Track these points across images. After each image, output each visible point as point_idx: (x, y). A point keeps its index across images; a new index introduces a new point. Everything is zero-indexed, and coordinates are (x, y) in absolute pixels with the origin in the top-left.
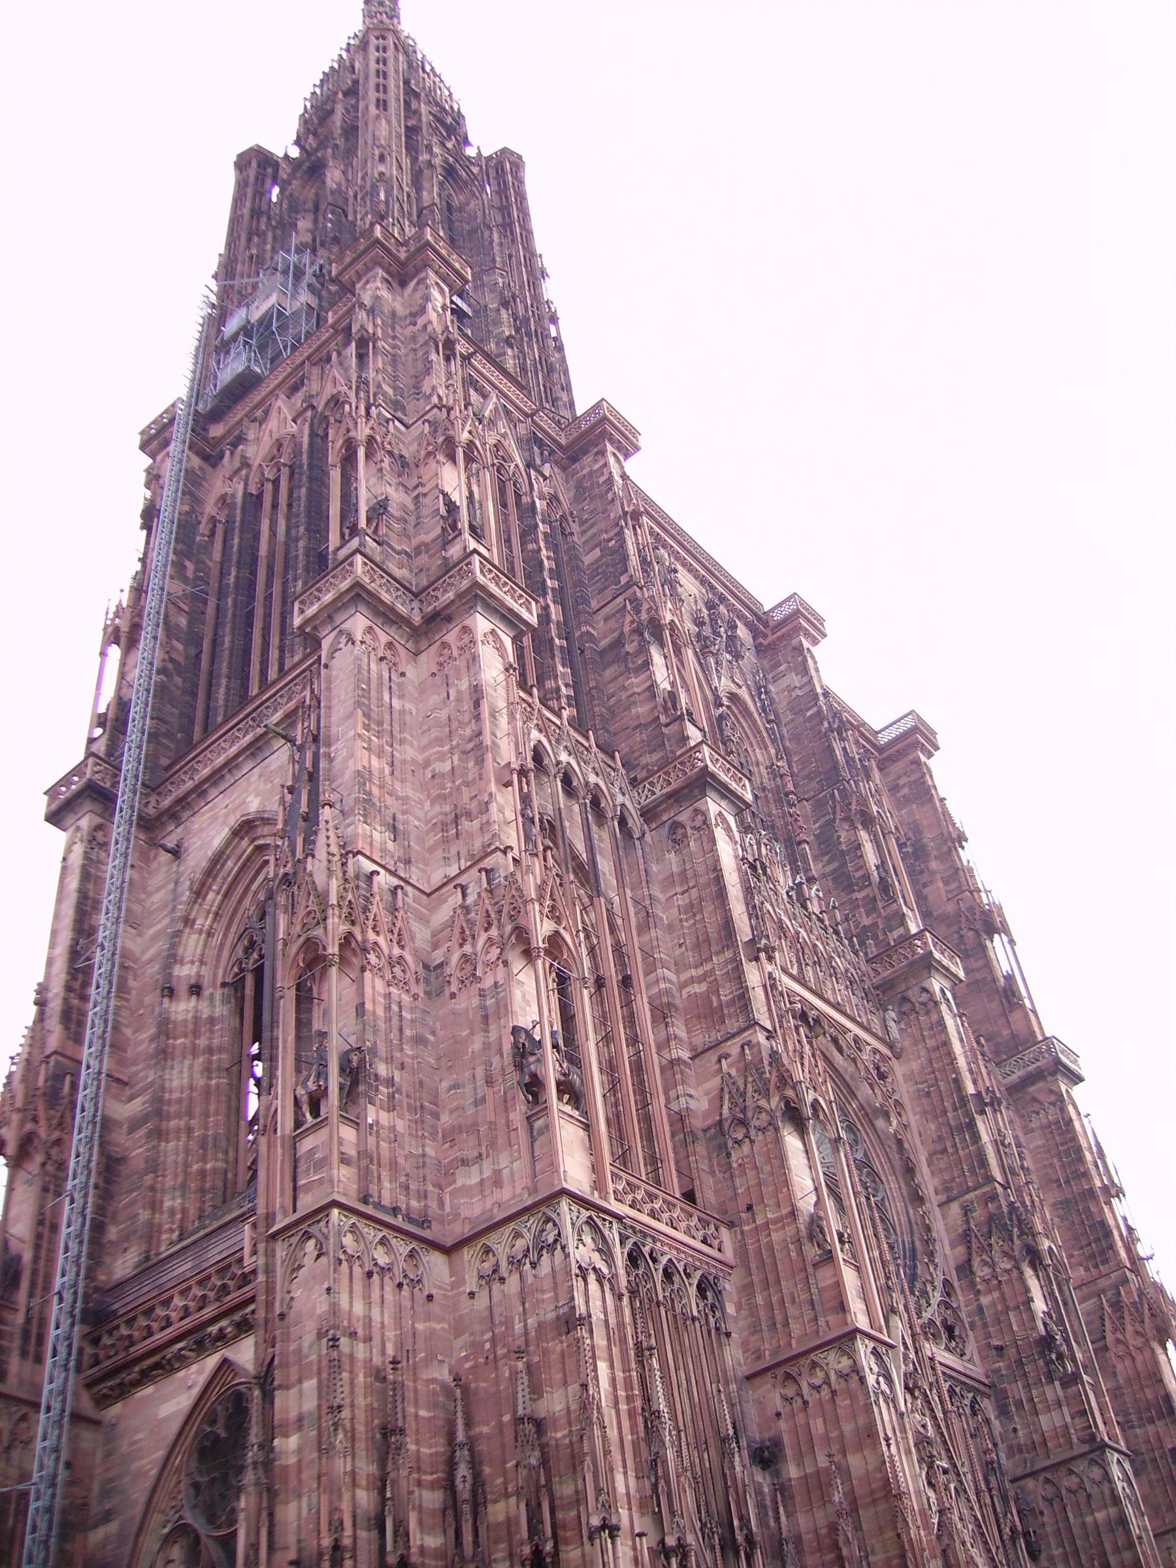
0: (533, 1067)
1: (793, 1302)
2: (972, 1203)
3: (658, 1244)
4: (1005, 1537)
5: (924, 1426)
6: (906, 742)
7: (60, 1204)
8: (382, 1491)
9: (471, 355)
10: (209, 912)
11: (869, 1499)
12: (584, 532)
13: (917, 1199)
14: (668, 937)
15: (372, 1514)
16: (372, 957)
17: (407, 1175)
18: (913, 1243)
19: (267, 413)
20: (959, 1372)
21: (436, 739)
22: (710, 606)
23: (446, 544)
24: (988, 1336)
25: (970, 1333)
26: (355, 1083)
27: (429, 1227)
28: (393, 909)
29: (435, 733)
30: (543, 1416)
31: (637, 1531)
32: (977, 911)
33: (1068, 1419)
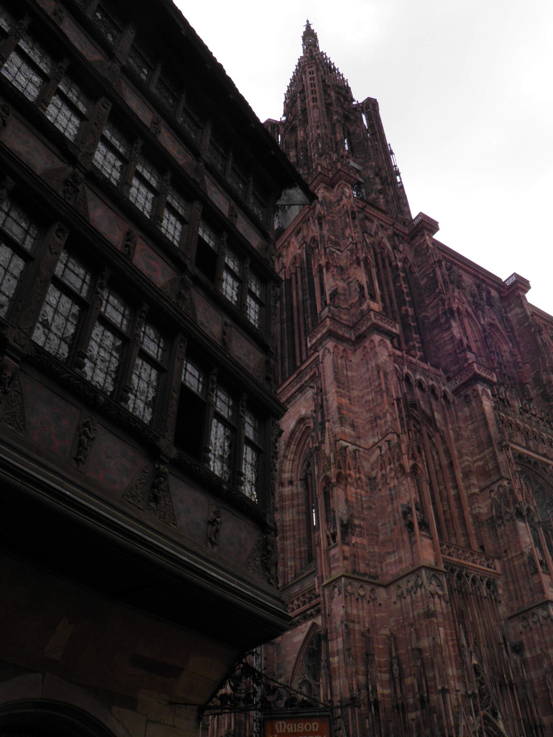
0: (410, 519)
1: (524, 588)
3: (469, 570)
8: (367, 676)
10: (292, 452)
12: (419, 271)
16: (349, 480)
17: (369, 560)
19: (289, 243)
22: (478, 287)
23: (361, 304)
26: (347, 528)
27: (378, 579)
28: (355, 459)
29: (365, 384)
30: (421, 647)
31: (457, 689)
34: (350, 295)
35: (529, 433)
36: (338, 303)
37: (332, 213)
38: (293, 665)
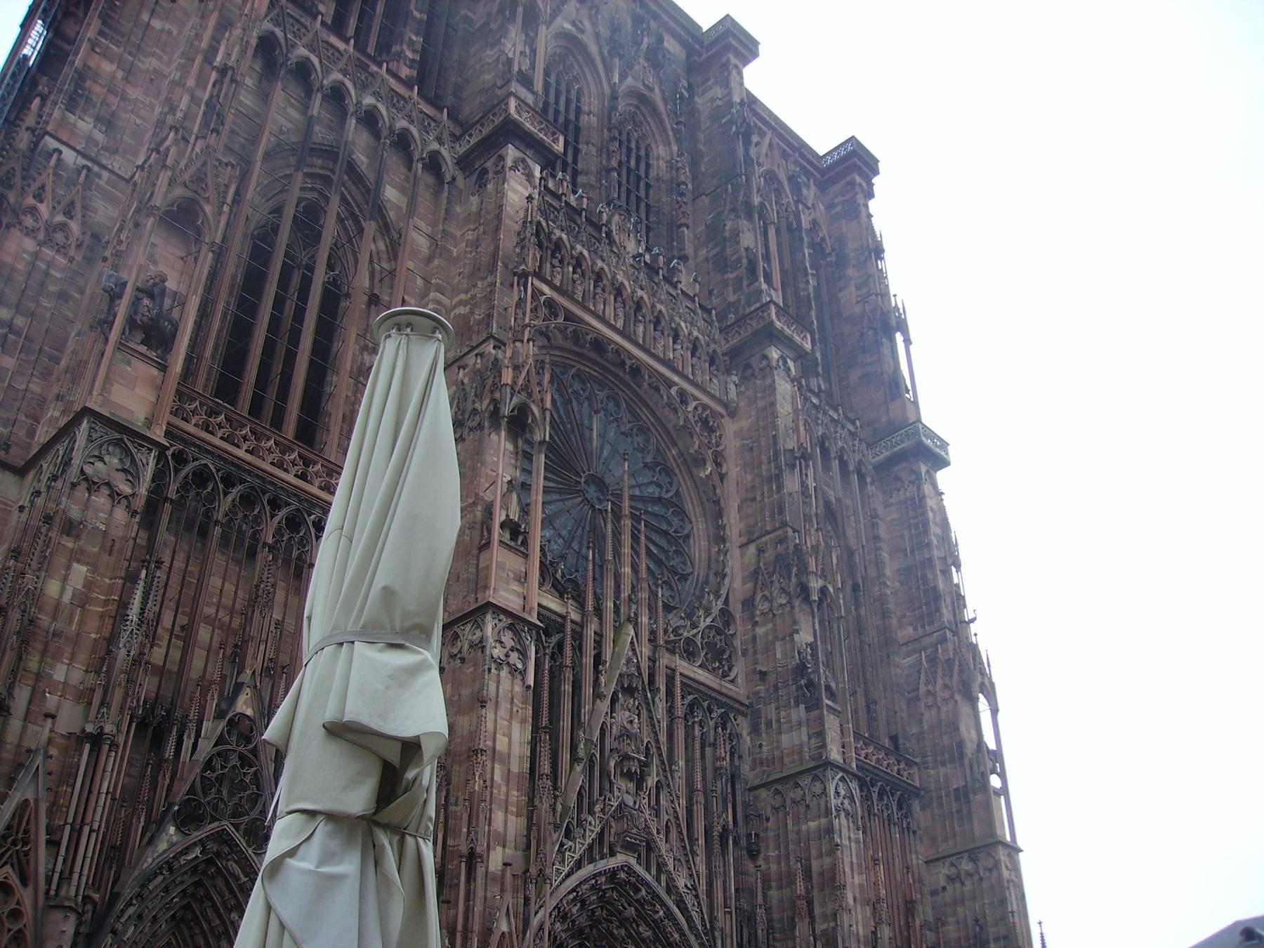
2: (766, 544)
5: (631, 722)
6: (845, 165)
13: (720, 538)
16: (29, 221)
18: (707, 576)
20: (714, 690)
22: (637, 20)
24: (756, 662)
32: (879, 312)
33: (805, 738)
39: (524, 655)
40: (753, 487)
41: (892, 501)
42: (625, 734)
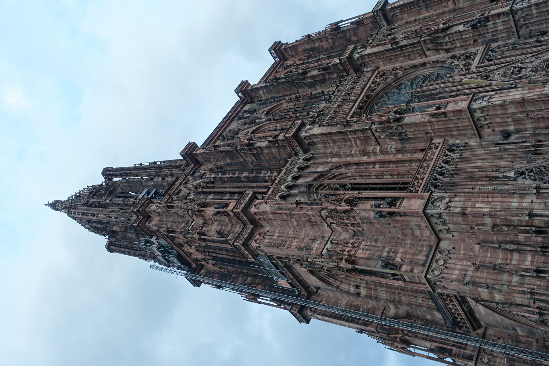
0: (385, 214)
4: (538, 44)
5: (499, 74)
7: (421, 334)
8: (513, 274)
9: (169, 195)
11: (524, 108)
12: (220, 161)
13: (424, 65)
14: (342, 149)
15: (520, 277)
16: (352, 253)
17: (416, 250)
18: (438, 67)
21: (287, 224)
22: (240, 118)
23: (229, 215)
25: (469, 50)
29: (285, 224)
30: (492, 224)
32: (332, 33)
33: (500, 20)
34: (223, 221)
35: (345, 98)
36: (227, 231)
37: (167, 221)
38: (505, 319)
39: (484, 97)
40: (405, 56)
41: (401, 17)
42: (504, 75)
